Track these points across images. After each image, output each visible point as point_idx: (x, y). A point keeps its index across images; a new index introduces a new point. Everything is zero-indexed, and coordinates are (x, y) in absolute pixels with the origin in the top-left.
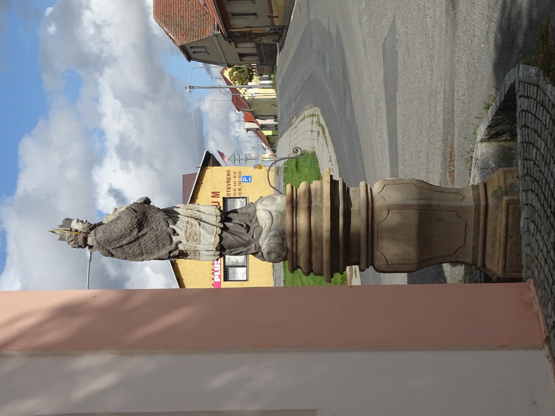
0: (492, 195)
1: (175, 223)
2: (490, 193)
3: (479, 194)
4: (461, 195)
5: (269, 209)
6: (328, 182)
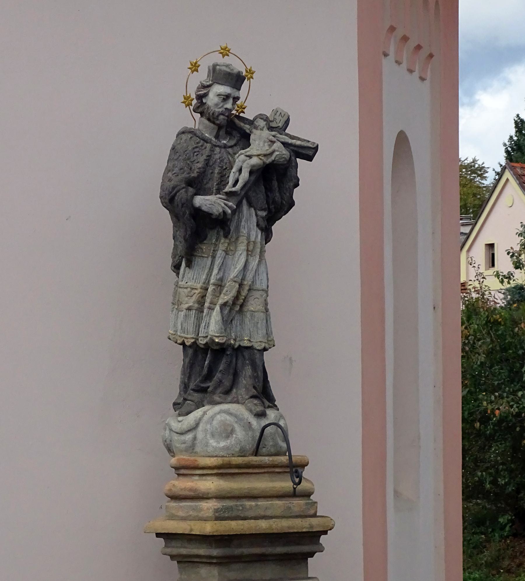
5: (200, 428)
6: (191, 530)
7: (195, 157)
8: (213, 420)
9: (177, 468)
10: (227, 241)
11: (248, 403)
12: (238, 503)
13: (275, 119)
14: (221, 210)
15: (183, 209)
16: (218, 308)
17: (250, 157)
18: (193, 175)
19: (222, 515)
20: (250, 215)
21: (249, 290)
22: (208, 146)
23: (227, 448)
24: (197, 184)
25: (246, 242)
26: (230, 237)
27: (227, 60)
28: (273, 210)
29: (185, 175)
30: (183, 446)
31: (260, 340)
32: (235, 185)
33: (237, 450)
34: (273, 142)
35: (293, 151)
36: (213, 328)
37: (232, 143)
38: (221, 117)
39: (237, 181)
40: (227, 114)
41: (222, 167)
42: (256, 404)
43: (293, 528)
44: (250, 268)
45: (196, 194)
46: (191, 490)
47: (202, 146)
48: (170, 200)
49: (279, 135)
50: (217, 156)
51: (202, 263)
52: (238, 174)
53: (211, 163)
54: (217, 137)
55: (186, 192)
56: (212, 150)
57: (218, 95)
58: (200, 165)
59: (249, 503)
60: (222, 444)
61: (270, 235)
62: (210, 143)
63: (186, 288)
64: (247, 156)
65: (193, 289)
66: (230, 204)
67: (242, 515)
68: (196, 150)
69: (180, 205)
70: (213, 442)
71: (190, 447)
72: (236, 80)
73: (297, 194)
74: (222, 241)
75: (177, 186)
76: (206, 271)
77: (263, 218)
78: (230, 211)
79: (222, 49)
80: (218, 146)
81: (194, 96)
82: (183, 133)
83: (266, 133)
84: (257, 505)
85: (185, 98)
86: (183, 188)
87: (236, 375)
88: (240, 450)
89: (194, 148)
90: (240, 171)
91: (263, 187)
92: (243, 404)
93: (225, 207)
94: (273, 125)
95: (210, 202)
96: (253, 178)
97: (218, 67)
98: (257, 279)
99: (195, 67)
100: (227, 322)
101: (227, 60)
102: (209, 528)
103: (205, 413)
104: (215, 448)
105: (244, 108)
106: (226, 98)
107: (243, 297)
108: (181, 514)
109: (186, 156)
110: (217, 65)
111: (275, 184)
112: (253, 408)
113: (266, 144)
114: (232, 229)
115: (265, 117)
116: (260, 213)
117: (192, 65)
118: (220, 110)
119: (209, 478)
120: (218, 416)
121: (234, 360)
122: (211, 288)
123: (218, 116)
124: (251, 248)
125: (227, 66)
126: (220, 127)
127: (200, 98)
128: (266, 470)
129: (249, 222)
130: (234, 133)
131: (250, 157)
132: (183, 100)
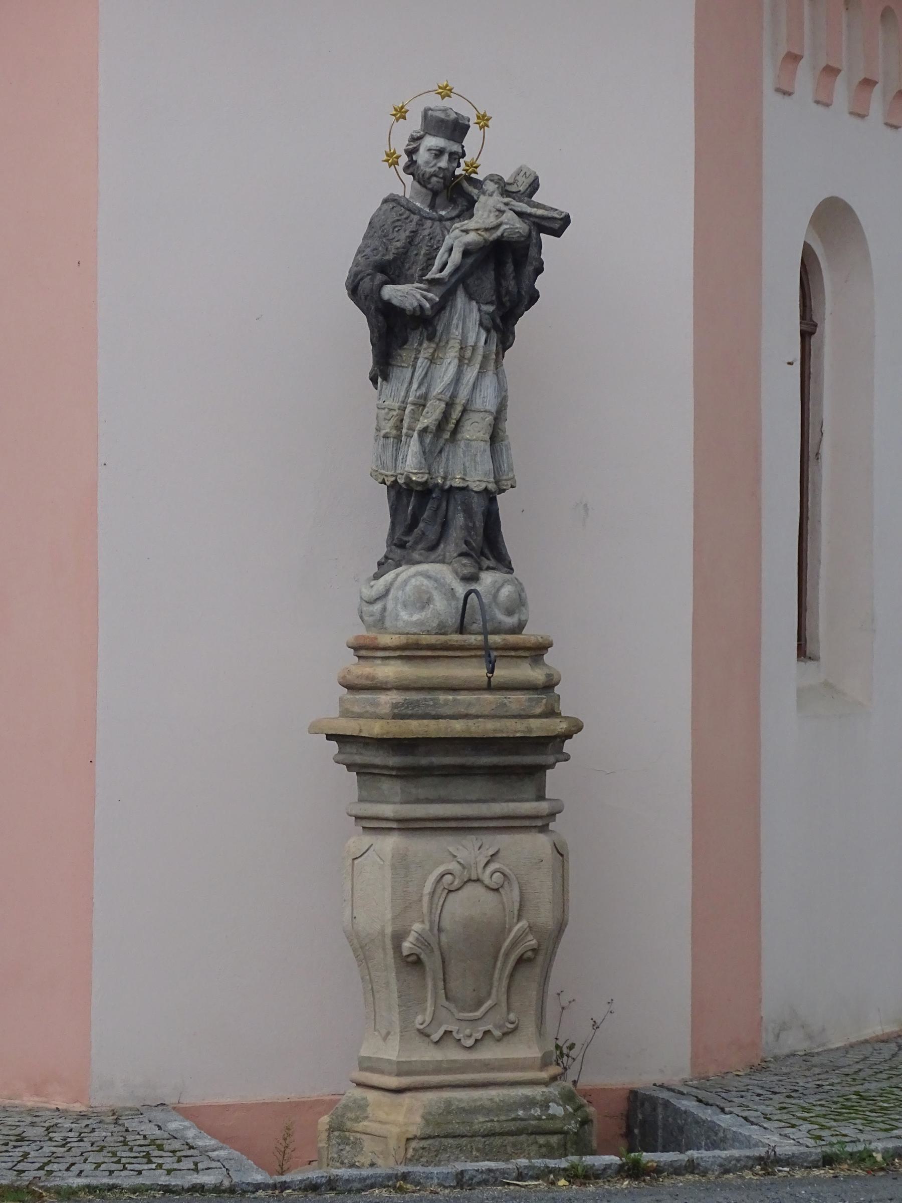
0: (365, 1099)
1: (386, 378)
2: (372, 1095)
3: (382, 1072)
4: (388, 1033)
7: (395, 234)
8: (406, 585)
9: (356, 648)
10: (433, 345)
11: (456, 562)
12: (429, 697)
13: (515, 181)
14: (416, 304)
15: (367, 303)
16: (416, 434)
17: (466, 232)
18: (387, 257)
20: (471, 311)
21: (464, 411)
22: (416, 218)
23: (421, 623)
24: (392, 269)
25: (458, 346)
26: (437, 340)
27: (447, 103)
28: (508, 304)
29: (378, 258)
30: (372, 618)
31: (480, 478)
32: (441, 270)
33: (435, 625)
34: (502, 212)
35: (534, 223)
36: (411, 463)
37: (454, 214)
38: (434, 179)
39: (445, 265)
40: (441, 176)
41: (432, 246)
42: (464, 565)
43: (502, 731)
44: (465, 381)
45: (386, 283)
46: (367, 678)
47: (407, 218)
48: (354, 291)
49: (514, 202)
50: (426, 232)
51: (401, 375)
52: (446, 255)
53: (417, 240)
54: (432, 206)
55: (372, 280)
56: (420, 224)
57: (429, 150)
58: (398, 244)
59: (442, 697)
60: (416, 617)
61: (511, 338)
62: (419, 214)
63: (384, 409)
64: (463, 231)
65: (391, 410)
66: (430, 295)
67: (433, 713)
68: (397, 224)
69: (363, 297)
70: (404, 615)
71: (379, 620)
72: (456, 129)
73: (540, 283)
74: (425, 345)
75: (361, 272)
76: (406, 385)
78: (428, 305)
79: (440, 88)
80: (430, 219)
81: (401, 151)
82: (385, 201)
83: (497, 200)
84: (455, 700)
85: (387, 155)
86: (368, 275)
87: (445, 525)
88: (439, 625)
89: (394, 222)
90: (451, 250)
91: (493, 273)
92: (450, 564)
93: (422, 299)
94: (513, 188)
95: (404, 294)
96: (470, 261)
97: (430, 112)
99: (401, 113)
100: (430, 455)
101: (447, 103)
102: (376, 729)
103: (398, 575)
104: (407, 623)
105: (476, 167)
106: (439, 153)
107: (454, 421)
108: (356, 709)
109: (383, 231)
110: (430, 109)
111: (510, 268)
112: (459, 570)
113: (492, 215)
114: (440, 329)
115: (496, 178)
116: (485, 308)
117: (396, 110)
118: (432, 170)
119: (392, 662)
120: (413, 580)
121: (444, 504)
122: (409, 408)
123: (429, 178)
124: (468, 354)
125: (445, 110)
126: (435, 194)
127: (410, 153)
128: (472, 653)
129: (467, 320)
130: (460, 200)
131: (466, 232)
132: (385, 158)
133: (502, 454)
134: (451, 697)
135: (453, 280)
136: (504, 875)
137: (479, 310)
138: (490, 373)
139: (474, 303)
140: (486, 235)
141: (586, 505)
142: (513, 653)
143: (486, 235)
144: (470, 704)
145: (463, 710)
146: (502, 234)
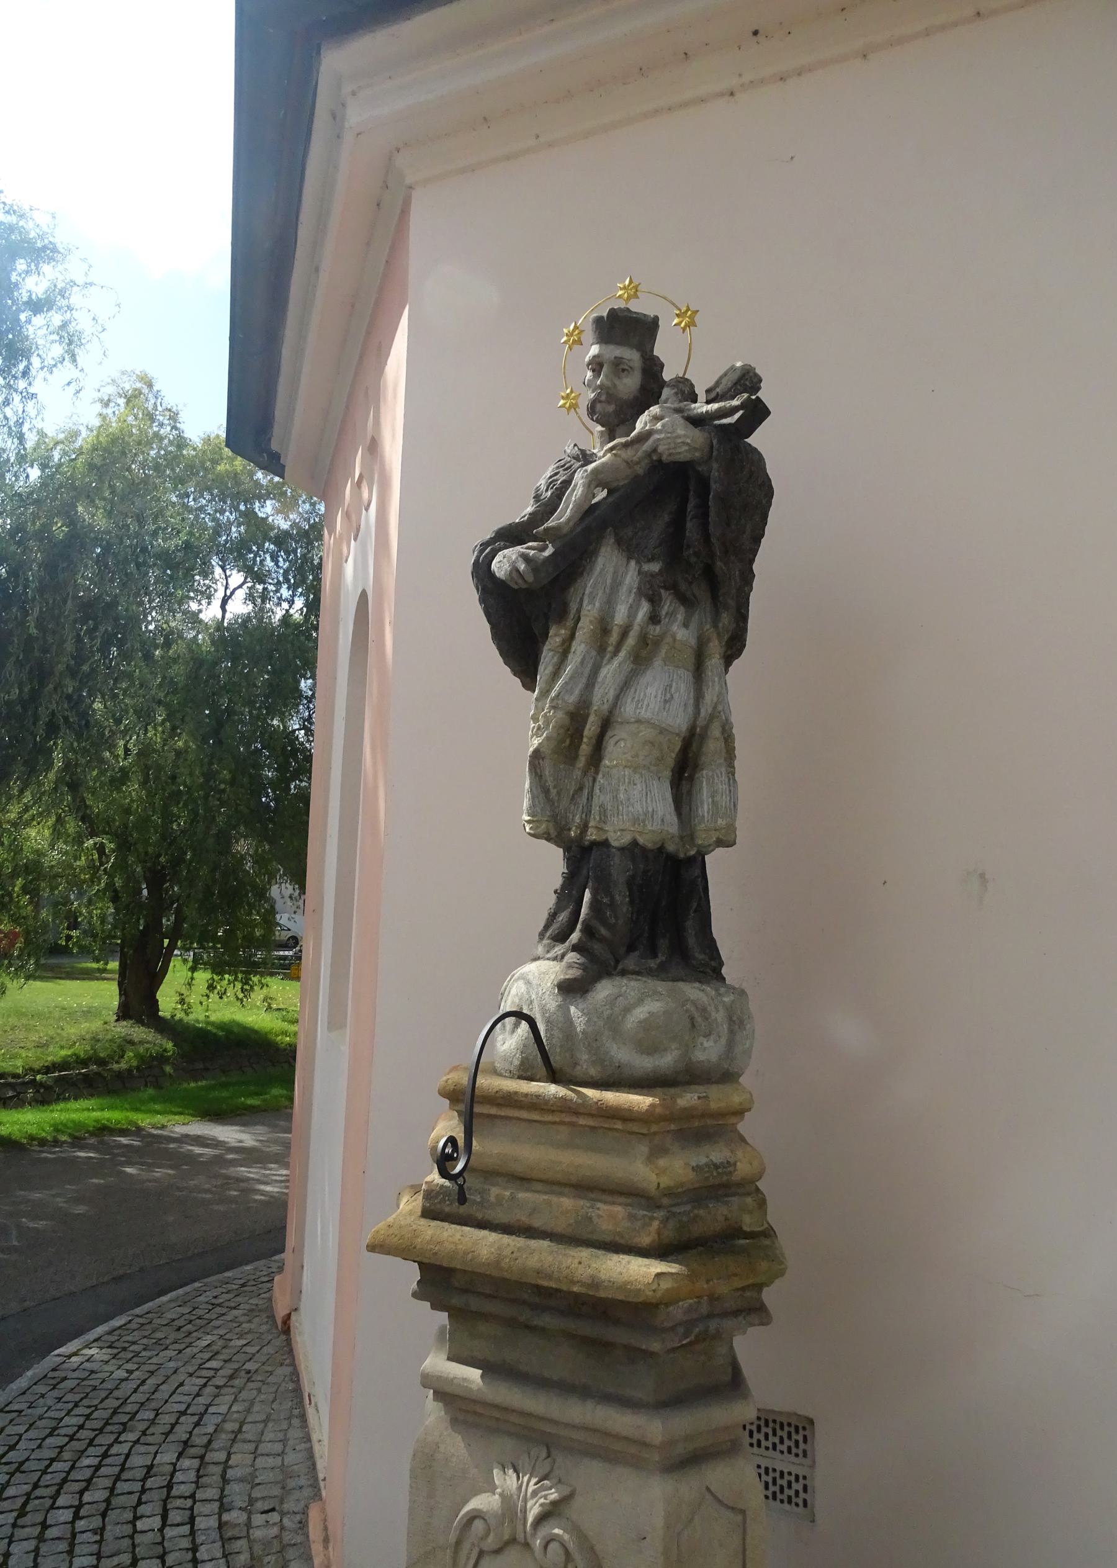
19: (438, 1206)
26: (570, 623)
33: (516, 1062)
43: (549, 1277)
67: (479, 1216)
77: (653, 575)
84: (513, 1198)
88: (522, 1063)
98: (629, 700)
114: (573, 607)
116: (646, 567)
124: (614, 638)
133: (701, 788)
134: (507, 1193)
135: (579, 529)
136: (567, 1553)
137: (640, 573)
138: (658, 663)
139: (633, 563)
140: (628, 454)
141: (982, 876)
142: (619, 1125)
143: (628, 454)
144: (534, 1211)
145: (521, 1217)
146: (655, 450)
